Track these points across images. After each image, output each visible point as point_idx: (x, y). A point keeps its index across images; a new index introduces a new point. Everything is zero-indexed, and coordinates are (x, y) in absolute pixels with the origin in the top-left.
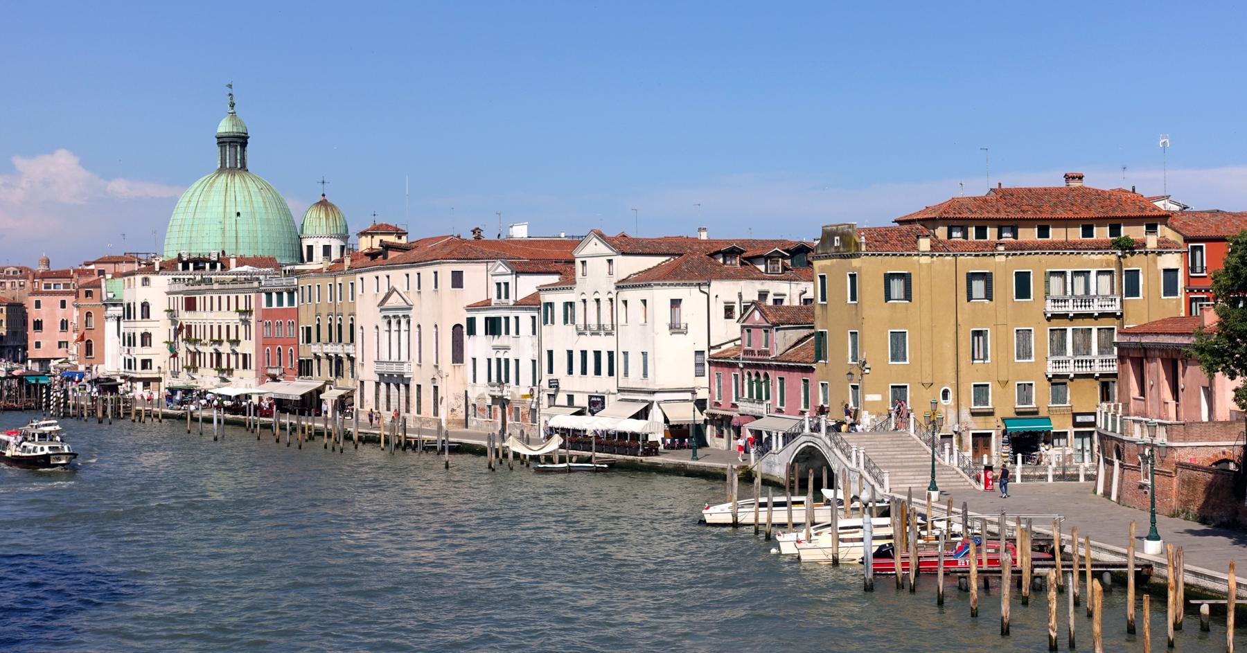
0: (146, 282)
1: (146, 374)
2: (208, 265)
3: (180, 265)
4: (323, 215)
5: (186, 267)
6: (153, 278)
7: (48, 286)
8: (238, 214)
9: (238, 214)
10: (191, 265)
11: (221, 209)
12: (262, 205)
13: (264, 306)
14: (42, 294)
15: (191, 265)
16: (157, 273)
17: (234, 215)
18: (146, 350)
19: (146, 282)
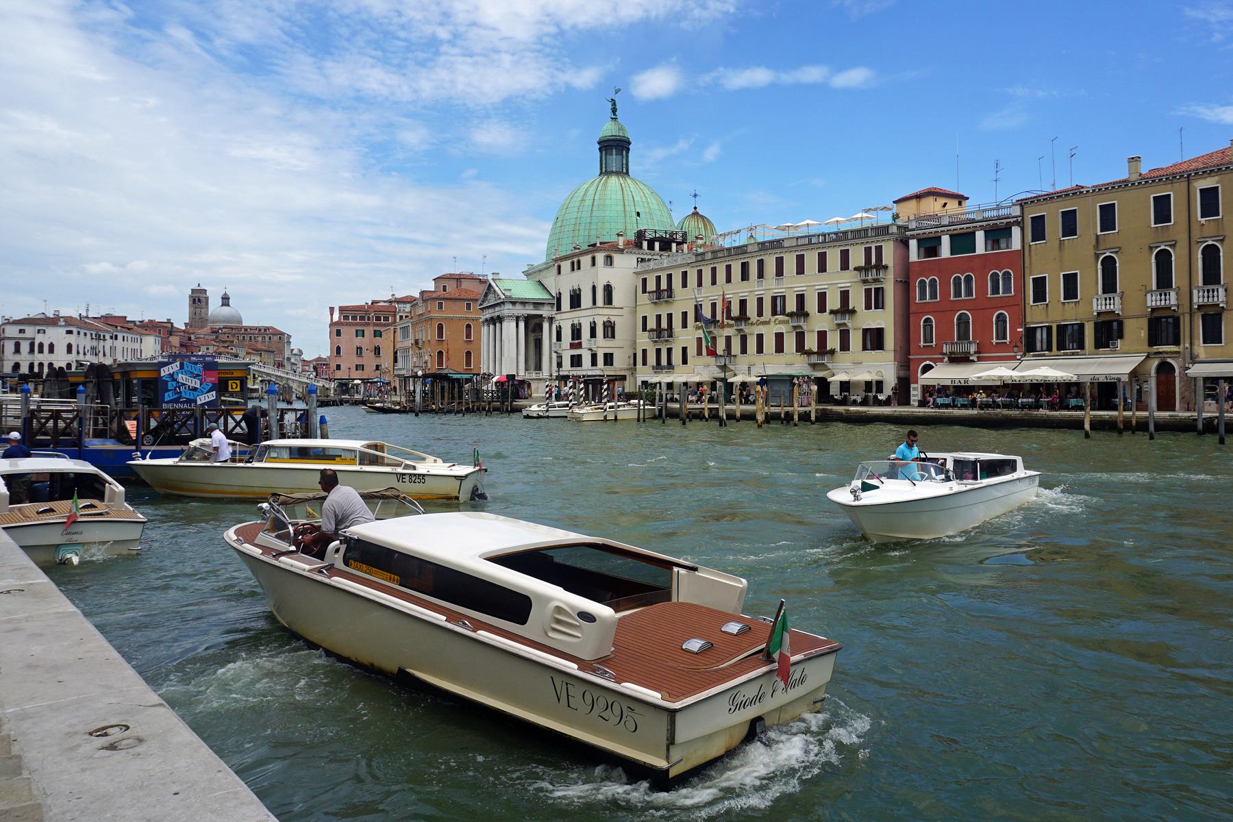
1: (609, 371)
2: (674, 245)
3: (645, 244)
4: (701, 225)
5: (651, 247)
6: (617, 258)
7: (346, 318)
8: (638, 214)
9: (638, 214)
10: (657, 245)
13: (914, 256)
15: (657, 245)
16: (621, 251)
17: (634, 214)
18: (610, 343)
19: (609, 261)
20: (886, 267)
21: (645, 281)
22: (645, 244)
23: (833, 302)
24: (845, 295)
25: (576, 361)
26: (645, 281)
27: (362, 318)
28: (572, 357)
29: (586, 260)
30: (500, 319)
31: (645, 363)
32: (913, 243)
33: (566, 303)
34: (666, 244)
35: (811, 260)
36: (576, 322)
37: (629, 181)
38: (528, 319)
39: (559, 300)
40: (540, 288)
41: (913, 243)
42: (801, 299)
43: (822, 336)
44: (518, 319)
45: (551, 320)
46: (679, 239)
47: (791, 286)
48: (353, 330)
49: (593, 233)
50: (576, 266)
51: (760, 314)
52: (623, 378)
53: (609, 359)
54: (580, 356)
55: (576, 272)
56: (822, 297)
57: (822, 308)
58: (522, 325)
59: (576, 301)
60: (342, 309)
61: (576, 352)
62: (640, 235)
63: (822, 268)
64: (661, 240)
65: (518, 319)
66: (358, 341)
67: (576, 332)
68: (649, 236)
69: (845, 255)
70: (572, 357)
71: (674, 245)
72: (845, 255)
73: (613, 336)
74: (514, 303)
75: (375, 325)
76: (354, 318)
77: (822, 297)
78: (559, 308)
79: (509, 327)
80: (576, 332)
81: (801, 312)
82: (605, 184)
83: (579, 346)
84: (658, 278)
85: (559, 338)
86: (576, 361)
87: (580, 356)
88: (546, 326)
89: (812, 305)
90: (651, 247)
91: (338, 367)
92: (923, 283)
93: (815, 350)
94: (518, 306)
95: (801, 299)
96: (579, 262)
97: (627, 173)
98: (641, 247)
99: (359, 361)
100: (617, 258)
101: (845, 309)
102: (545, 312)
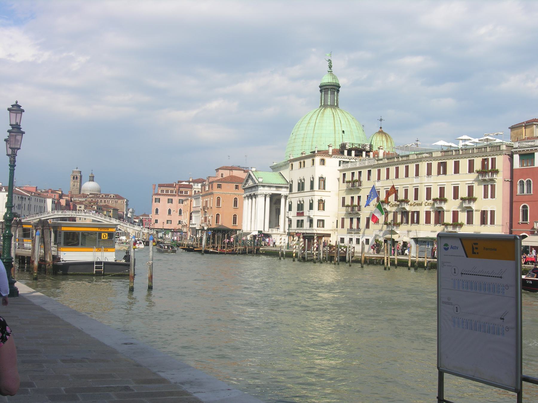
0: (323, 162)
1: (321, 231)
2: (364, 153)
3: (346, 152)
4: (384, 139)
5: (349, 154)
6: (327, 160)
7: (162, 191)
8: (343, 132)
9: (343, 132)
10: (353, 153)
11: (333, 128)
12: (355, 128)
14: (160, 195)
15: (353, 153)
17: (341, 132)
18: (321, 213)
19: (323, 162)
20: (497, 172)
21: (344, 175)
22: (346, 152)
23: (463, 193)
24: (471, 189)
25: (300, 224)
26: (344, 175)
27: (172, 191)
28: (298, 221)
29: (308, 162)
30: (255, 196)
31: (343, 226)
32: (516, 157)
33: (295, 188)
34: (359, 152)
35: (450, 165)
36: (301, 199)
37: (338, 110)
38: (272, 196)
39: (291, 186)
40: (280, 177)
41: (516, 157)
42: (442, 190)
43: (455, 214)
44: (266, 196)
45: (286, 197)
46: (368, 148)
47: (435, 182)
48: (166, 198)
49: (314, 143)
50: (302, 165)
51: (416, 198)
52: (329, 235)
53: (321, 222)
54: (302, 221)
55: (302, 169)
56: (456, 190)
57: (456, 196)
58: (268, 199)
59: (301, 187)
60: (160, 186)
61: (300, 218)
62: (343, 146)
63: (457, 171)
64: (356, 150)
65: (266, 196)
66: (169, 206)
67: (300, 207)
68: (348, 147)
69: (471, 164)
70: (298, 221)
71: (364, 153)
72: (471, 164)
73: (324, 209)
74: (264, 186)
75: (179, 196)
76: (167, 191)
77: (456, 190)
78: (291, 191)
79: (260, 200)
80: (300, 207)
81: (442, 199)
82: (323, 113)
83: (302, 214)
84: (353, 173)
85: (290, 209)
86: (300, 224)
87: (302, 221)
88: (283, 200)
89: (449, 194)
90: (349, 154)
91: (156, 221)
92: (522, 183)
93: (451, 222)
94: (266, 188)
95: (442, 190)
96: (304, 162)
97: (337, 106)
98: (342, 153)
99: (169, 218)
100: (327, 160)
101: (471, 198)
102: (284, 192)
